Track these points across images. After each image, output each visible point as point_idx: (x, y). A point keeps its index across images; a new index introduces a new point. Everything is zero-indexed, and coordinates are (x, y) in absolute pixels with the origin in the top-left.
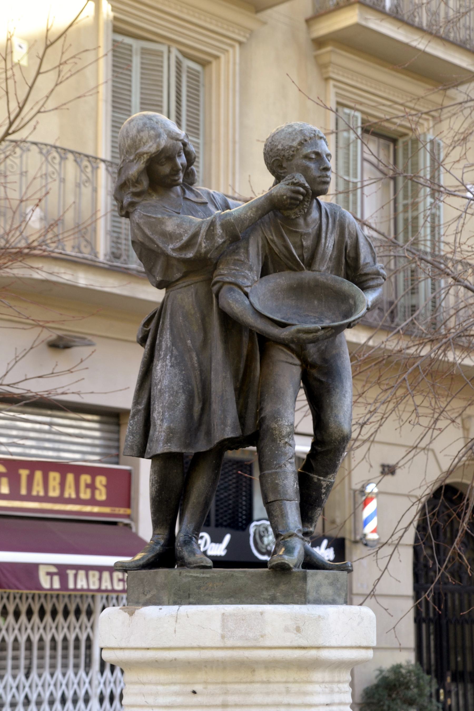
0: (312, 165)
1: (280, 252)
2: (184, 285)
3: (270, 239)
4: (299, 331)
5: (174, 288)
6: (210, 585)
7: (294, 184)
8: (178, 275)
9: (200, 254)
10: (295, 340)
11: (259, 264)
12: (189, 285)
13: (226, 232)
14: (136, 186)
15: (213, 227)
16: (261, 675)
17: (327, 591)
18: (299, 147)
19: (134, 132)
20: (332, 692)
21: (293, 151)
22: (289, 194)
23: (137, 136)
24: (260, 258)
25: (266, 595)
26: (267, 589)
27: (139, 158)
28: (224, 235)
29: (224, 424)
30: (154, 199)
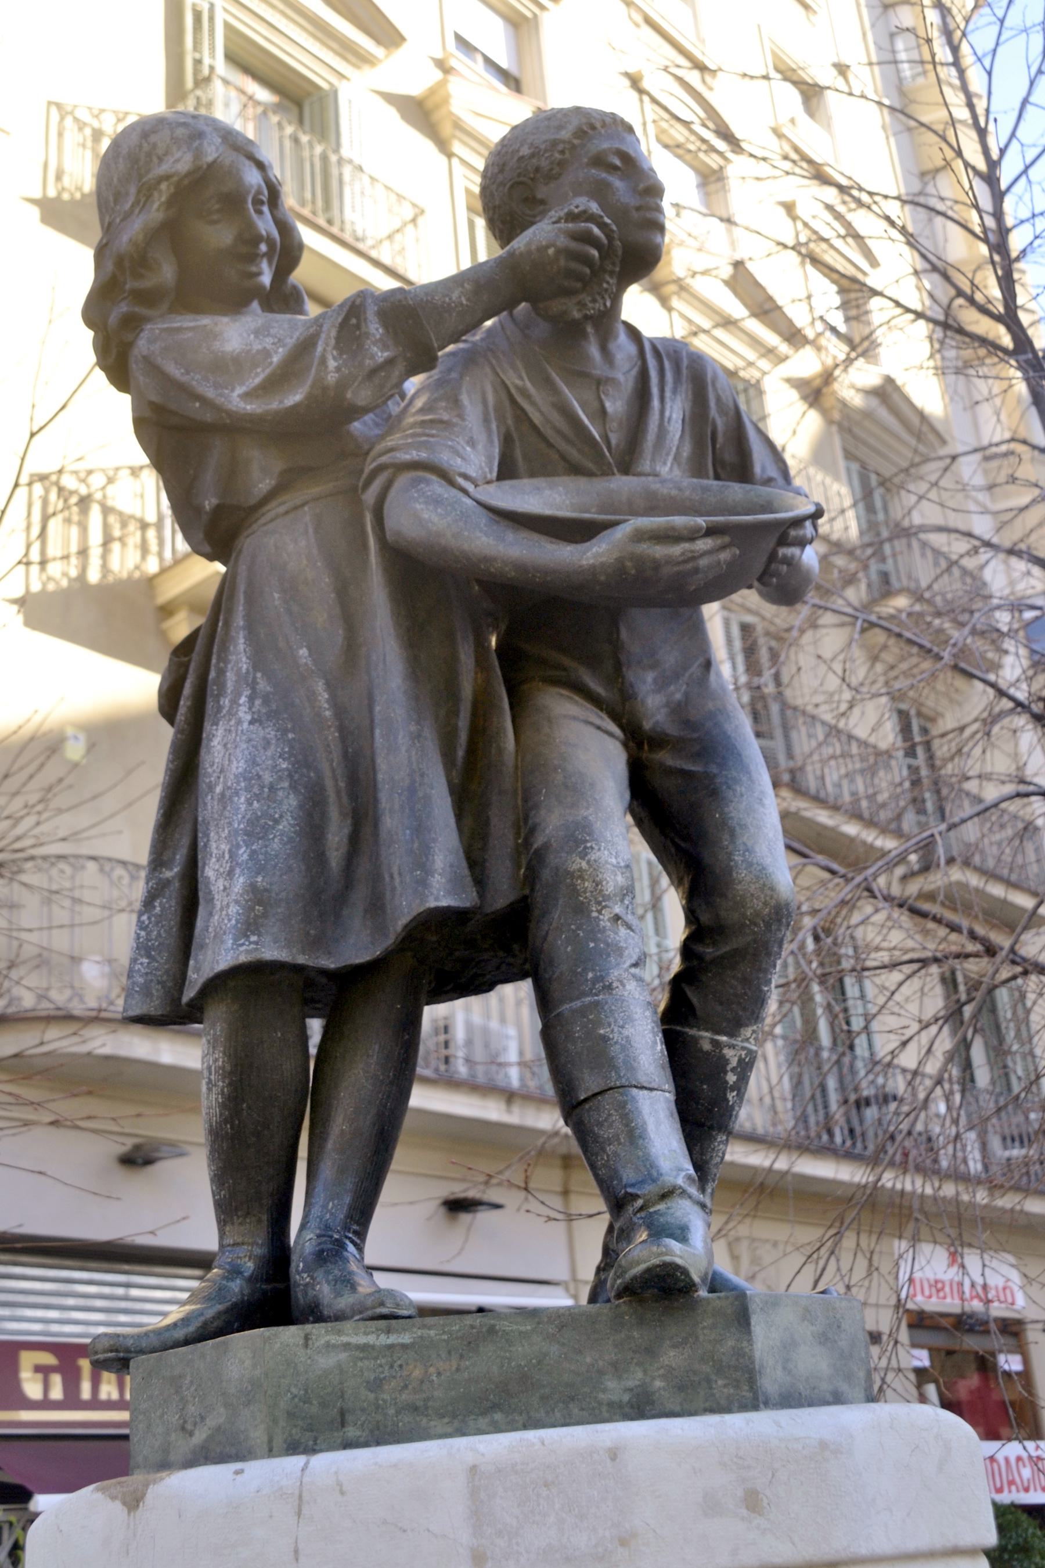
0: (618, 184)
1: (547, 420)
2: (282, 509)
3: (517, 387)
4: (639, 536)
6: (417, 1373)
7: (572, 217)
8: (264, 485)
9: (325, 389)
10: (629, 564)
11: (491, 442)
12: (296, 508)
14: (141, 276)
15: (358, 319)
21: (562, 152)
22: (563, 241)
23: (141, 146)
24: (494, 426)
25: (614, 1389)
26: (617, 1369)
27: (149, 197)
29: (422, 862)
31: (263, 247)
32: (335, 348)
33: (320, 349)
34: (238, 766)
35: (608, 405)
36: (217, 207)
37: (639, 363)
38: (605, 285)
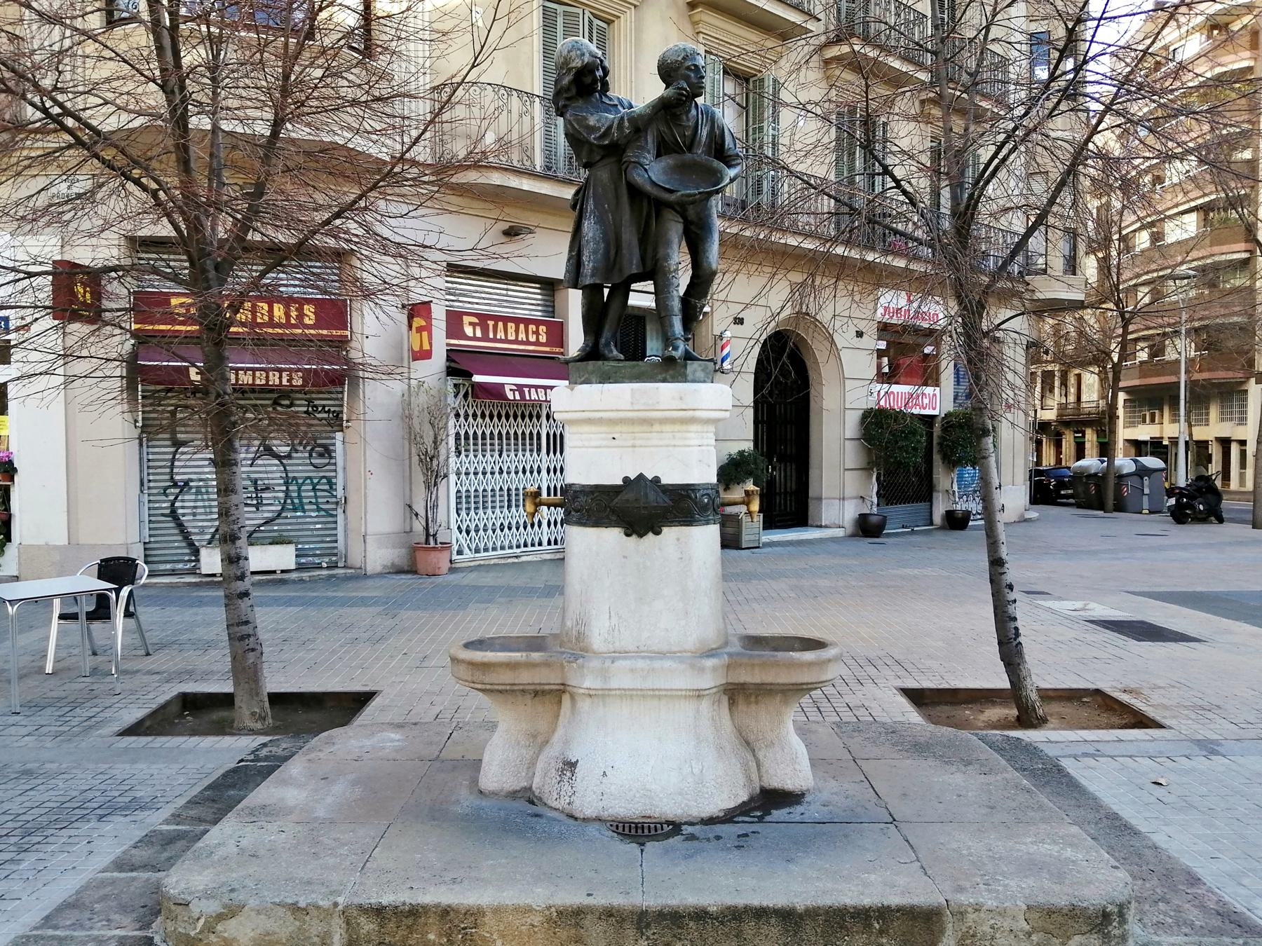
4: (682, 195)
7: (678, 88)
16: (657, 427)
17: (700, 374)
19: (565, 53)
20: (703, 438)
25: (660, 377)
26: (661, 374)
29: (631, 263)
30: (580, 103)
34: (591, 235)
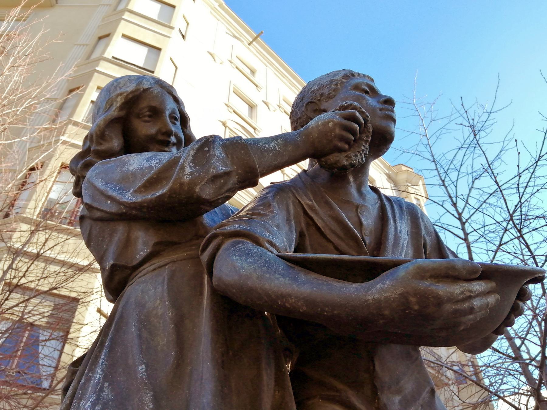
1: (327, 225)
2: (152, 268)
3: (307, 205)
5: (133, 281)
7: (343, 108)
9: (182, 184)
13: (232, 157)
14: (101, 144)
18: (344, 80)
21: (336, 85)
22: (338, 119)
24: (293, 223)
27: (111, 105)
28: (229, 163)
31: (173, 139)
32: (191, 162)
33: (181, 161)
35: (363, 220)
36: (148, 113)
37: (379, 202)
38: (362, 148)
